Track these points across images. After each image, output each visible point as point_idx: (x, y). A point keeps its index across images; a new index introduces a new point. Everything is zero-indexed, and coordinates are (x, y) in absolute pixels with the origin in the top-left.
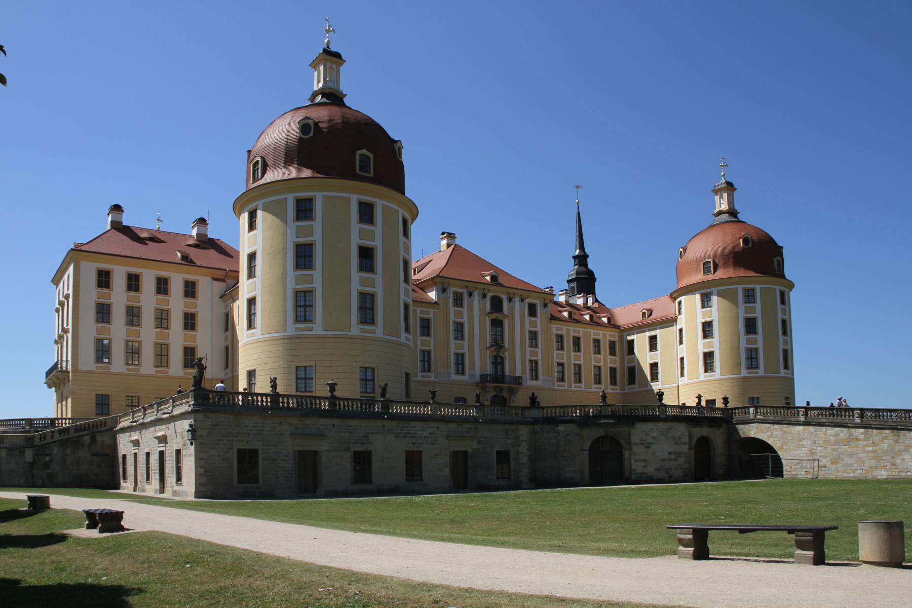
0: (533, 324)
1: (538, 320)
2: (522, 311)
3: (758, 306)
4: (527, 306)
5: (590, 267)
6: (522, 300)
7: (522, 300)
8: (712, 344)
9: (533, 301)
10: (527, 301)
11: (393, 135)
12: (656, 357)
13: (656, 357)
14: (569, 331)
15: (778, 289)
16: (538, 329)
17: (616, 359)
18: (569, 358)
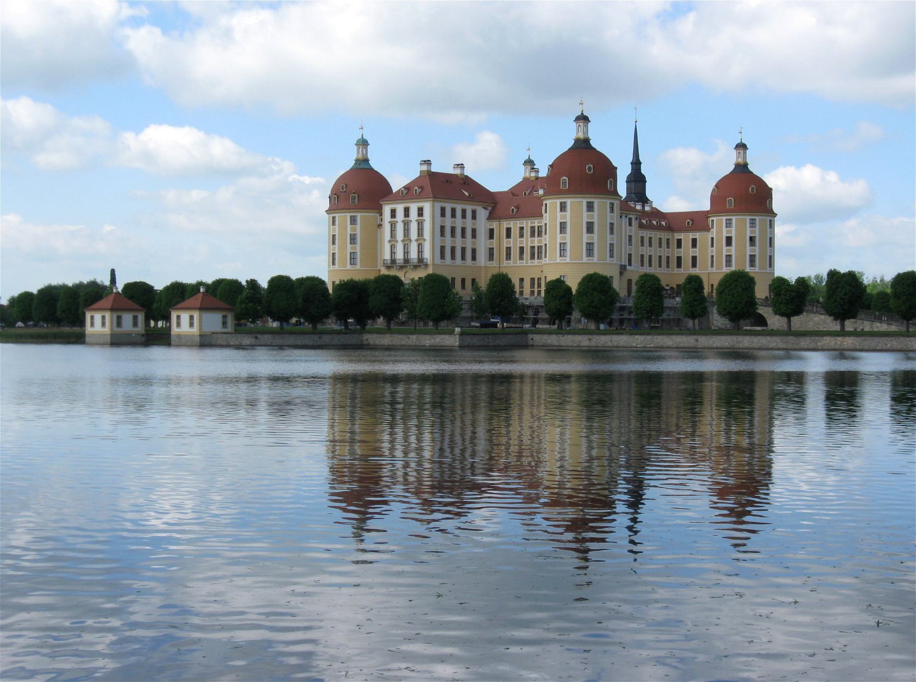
0: (630, 231)
1: (633, 228)
2: (626, 222)
3: (757, 229)
4: (628, 219)
5: (643, 172)
6: (626, 217)
7: (626, 217)
8: (730, 251)
9: (630, 216)
10: (628, 217)
11: (615, 164)
12: (697, 252)
13: (697, 252)
14: (647, 234)
15: (768, 218)
16: (633, 234)
17: (677, 254)
18: (647, 251)
